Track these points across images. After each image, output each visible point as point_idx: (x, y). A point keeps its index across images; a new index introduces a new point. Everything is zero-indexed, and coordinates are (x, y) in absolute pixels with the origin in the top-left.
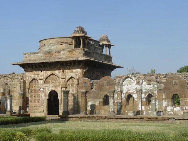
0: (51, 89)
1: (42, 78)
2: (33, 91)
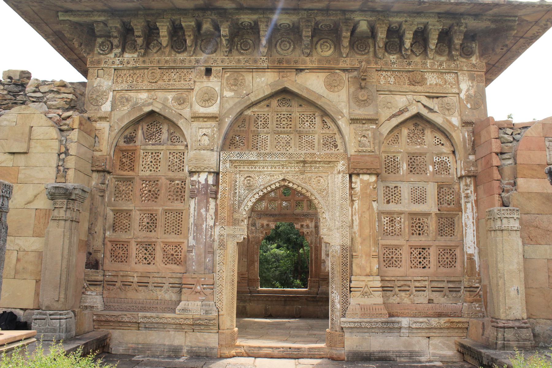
0: (268, 177)
1: (213, 109)
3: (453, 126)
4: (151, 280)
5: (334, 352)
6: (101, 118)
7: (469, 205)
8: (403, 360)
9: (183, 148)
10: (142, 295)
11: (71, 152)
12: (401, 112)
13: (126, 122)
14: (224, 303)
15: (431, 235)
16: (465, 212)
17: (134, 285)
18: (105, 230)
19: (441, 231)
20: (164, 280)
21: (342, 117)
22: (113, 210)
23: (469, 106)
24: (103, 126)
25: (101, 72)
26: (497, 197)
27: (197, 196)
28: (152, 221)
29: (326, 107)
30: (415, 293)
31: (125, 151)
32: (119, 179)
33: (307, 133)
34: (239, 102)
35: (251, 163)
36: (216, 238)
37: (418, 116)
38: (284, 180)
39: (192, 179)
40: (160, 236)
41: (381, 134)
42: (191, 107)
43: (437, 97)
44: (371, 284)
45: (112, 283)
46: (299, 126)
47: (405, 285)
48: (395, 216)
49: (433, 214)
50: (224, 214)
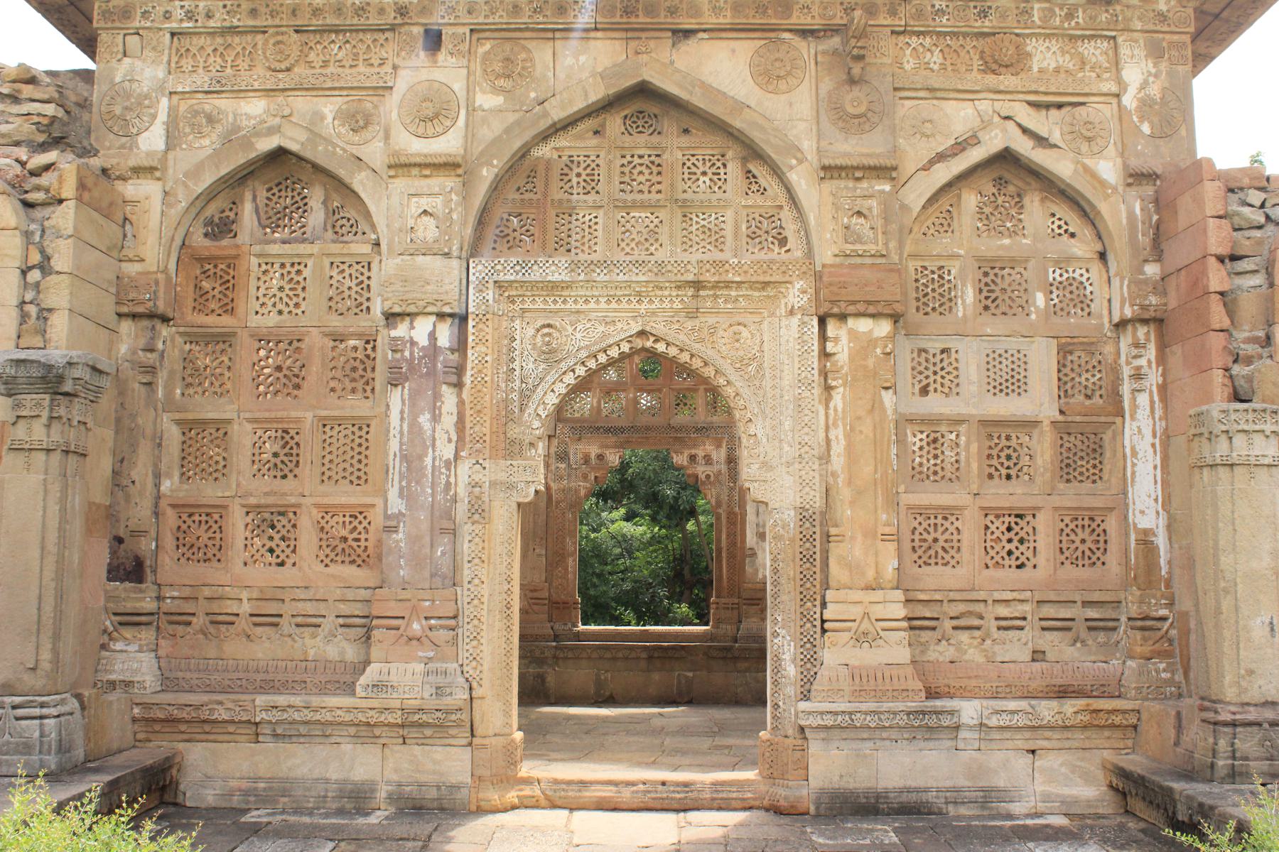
0: (598, 326)
1: (448, 144)
3: (1103, 183)
4: (287, 609)
5: (782, 792)
6: (138, 171)
7: (1143, 399)
8: (963, 811)
9: (367, 249)
10: (265, 649)
11: (58, 263)
12: (960, 147)
13: (208, 179)
14: (486, 667)
15: (1039, 480)
16: (1133, 418)
17: (243, 624)
18: (158, 476)
19: (1067, 469)
20: (322, 608)
21: (800, 162)
22: (179, 422)
23: (1146, 128)
24: (144, 191)
25: (133, 41)
26: (1218, 376)
27: (407, 379)
28: (286, 450)
29: (756, 136)
30: (996, 634)
31: (209, 259)
32: (192, 338)
33: (704, 207)
34: (518, 123)
35: (554, 288)
36: (462, 491)
37: (1006, 157)
38: (642, 334)
39: (394, 333)
40: (309, 491)
41: (904, 208)
42: (387, 137)
43: (1060, 106)
44: (878, 611)
45: (181, 619)
46: (681, 186)
47: (970, 613)
48: (943, 429)
49: (1046, 422)
50: (483, 427)
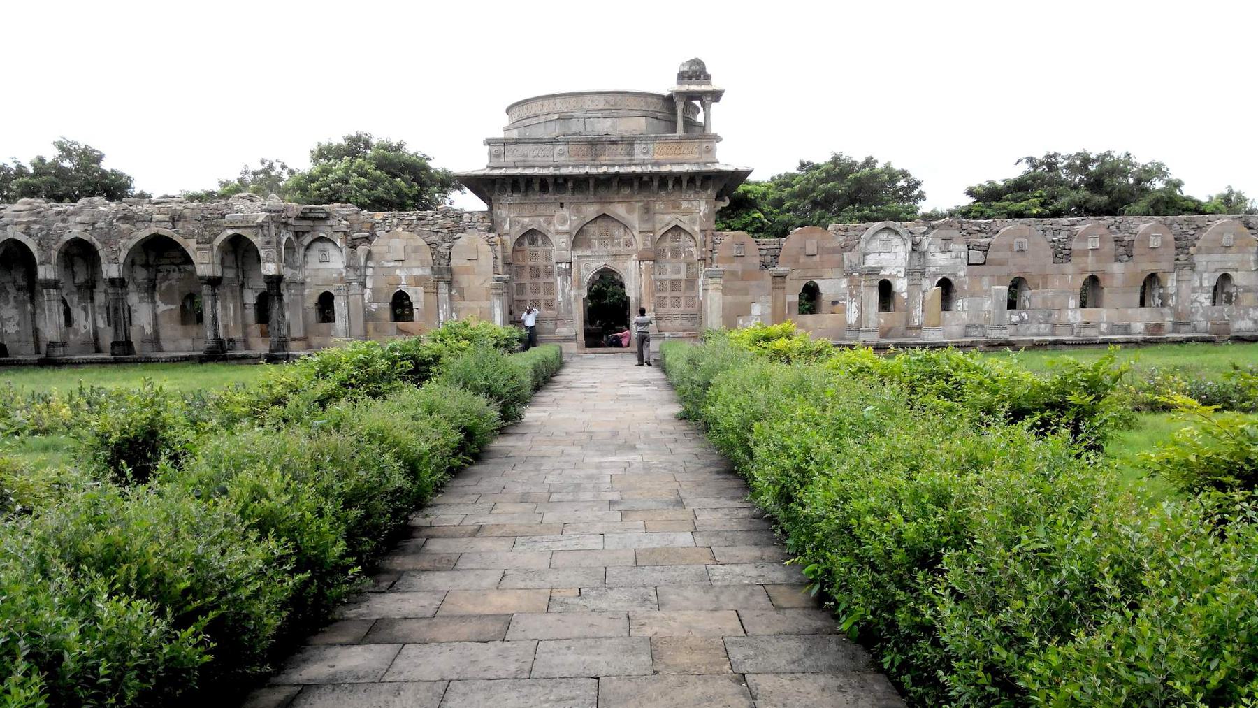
0: (598, 265)
1: (566, 228)
2: (528, 270)
19: (687, 288)
40: (542, 296)
